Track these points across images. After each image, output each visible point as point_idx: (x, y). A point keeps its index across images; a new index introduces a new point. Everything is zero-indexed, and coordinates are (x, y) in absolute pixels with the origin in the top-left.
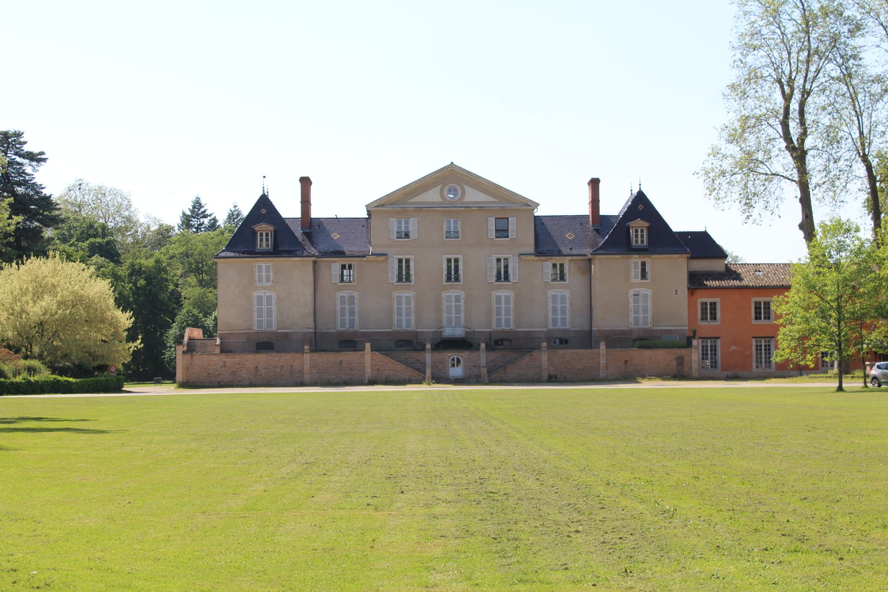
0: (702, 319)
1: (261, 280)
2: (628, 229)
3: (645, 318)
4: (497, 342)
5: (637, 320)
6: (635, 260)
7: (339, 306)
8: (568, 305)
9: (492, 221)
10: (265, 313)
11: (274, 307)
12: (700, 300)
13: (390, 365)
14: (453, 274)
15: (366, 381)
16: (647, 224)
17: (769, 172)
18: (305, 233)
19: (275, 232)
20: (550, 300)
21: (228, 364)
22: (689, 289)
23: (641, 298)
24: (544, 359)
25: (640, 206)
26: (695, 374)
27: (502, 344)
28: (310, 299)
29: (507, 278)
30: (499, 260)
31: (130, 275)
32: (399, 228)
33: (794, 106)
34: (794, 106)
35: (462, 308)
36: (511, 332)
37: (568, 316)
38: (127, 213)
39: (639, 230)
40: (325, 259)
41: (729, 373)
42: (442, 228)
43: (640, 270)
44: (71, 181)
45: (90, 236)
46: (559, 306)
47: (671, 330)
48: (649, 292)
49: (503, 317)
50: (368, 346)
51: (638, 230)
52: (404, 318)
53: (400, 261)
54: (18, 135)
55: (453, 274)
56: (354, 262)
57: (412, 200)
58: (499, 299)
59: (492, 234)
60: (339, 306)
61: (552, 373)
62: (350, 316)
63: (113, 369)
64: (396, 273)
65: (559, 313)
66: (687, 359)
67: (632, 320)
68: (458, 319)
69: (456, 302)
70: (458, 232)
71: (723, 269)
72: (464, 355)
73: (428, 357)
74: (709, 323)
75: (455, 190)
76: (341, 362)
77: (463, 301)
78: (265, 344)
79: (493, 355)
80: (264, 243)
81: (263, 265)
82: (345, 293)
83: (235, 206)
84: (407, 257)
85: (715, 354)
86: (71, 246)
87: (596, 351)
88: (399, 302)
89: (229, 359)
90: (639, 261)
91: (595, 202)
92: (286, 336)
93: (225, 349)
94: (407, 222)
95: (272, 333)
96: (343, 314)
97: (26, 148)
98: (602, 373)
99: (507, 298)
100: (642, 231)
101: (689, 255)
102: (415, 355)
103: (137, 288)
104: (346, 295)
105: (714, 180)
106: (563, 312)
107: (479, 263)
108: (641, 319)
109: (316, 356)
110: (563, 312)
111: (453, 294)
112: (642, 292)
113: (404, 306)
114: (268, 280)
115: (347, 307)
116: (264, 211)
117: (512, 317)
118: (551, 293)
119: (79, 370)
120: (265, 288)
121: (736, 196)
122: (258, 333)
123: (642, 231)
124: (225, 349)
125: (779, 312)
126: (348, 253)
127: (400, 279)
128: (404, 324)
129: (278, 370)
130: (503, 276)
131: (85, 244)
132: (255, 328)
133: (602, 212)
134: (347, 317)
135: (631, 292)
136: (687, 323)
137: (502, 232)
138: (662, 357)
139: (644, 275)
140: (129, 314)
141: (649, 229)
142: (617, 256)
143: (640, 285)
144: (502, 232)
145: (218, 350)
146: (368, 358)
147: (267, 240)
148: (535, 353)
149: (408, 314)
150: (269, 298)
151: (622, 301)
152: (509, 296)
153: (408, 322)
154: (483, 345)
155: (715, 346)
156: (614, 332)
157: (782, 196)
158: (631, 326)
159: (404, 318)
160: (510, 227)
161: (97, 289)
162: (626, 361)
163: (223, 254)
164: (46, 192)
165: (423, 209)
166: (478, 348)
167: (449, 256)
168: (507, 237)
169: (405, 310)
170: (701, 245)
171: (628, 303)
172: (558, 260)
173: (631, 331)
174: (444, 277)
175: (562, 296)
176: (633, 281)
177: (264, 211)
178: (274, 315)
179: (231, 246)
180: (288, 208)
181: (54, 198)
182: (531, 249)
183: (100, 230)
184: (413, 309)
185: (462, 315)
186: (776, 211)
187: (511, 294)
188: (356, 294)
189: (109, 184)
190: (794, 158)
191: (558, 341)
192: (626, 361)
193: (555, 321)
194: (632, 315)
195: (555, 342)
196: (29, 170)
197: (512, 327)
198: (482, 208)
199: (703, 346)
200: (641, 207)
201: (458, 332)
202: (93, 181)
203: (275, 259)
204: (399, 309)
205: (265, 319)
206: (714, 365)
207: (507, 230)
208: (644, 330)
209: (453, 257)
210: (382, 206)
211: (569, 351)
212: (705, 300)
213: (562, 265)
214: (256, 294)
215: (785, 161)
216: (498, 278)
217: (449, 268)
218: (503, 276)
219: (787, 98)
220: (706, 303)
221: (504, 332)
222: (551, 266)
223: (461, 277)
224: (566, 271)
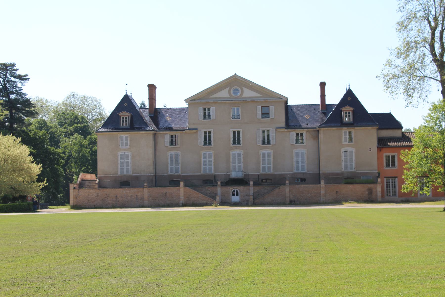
0: (387, 166)
1: (122, 145)
2: (341, 111)
3: (351, 166)
5: (346, 167)
6: (345, 130)
7: (169, 160)
8: (305, 158)
9: (259, 108)
11: (130, 161)
12: (385, 155)
13: (195, 195)
14: (236, 140)
15: (181, 204)
16: (352, 109)
17: (422, 75)
18: (151, 117)
19: (132, 117)
20: (295, 155)
21: (100, 195)
22: (378, 147)
23: (348, 154)
24: (287, 189)
25: (350, 98)
26: (380, 199)
28: (151, 156)
29: (268, 142)
30: (264, 132)
31: (89, 145)
33: (437, 34)
34: (437, 34)
35: (242, 160)
36: (271, 174)
37: (305, 165)
38: (98, 110)
40: (161, 132)
41: (403, 199)
42: (230, 113)
44: (69, 93)
45: (75, 123)
46: (300, 159)
47: (367, 173)
48: (354, 150)
49: (266, 165)
50: (182, 183)
51: (349, 112)
52: (208, 166)
53: (205, 133)
54: (13, 65)
56: (178, 134)
57: (212, 97)
58: (264, 155)
59: (260, 116)
60: (169, 160)
61: (292, 199)
62: (176, 165)
63: (29, 198)
65: (300, 163)
67: (343, 167)
68: (240, 167)
69: (238, 157)
70: (239, 115)
72: (240, 189)
73: (219, 190)
75: (238, 90)
77: (242, 156)
78: (125, 183)
79: (257, 188)
80: (124, 124)
81: (124, 136)
82: (173, 152)
83: (165, 106)
84: (210, 130)
85: (395, 187)
86: (65, 128)
87: (319, 185)
88: (205, 157)
89: (102, 192)
92: (137, 178)
93: (101, 186)
95: (129, 176)
97: (18, 73)
98: (323, 199)
100: (349, 113)
101: (378, 127)
102: (210, 189)
103: (93, 151)
105: (390, 80)
106: (303, 162)
107: (252, 133)
108: (349, 167)
109: (151, 189)
110: (303, 162)
111: (236, 152)
112: (349, 150)
113: (207, 160)
115: (174, 160)
116: (126, 104)
117: (272, 166)
118: (295, 151)
119: (5, 199)
120: (125, 150)
121: (402, 91)
122: (121, 176)
123: (349, 113)
124: (101, 186)
125: (405, 160)
126: (174, 129)
127: (205, 143)
128: (208, 170)
129: (129, 198)
130: (266, 141)
131: (72, 128)
132: (119, 173)
133: (327, 102)
134: (174, 166)
135: (343, 150)
136: (377, 168)
137: (265, 115)
138: (359, 189)
140: (40, 165)
141: (353, 112)
142: (334, 128)
143: (348, 146)
144: (265, 115)
145: (96, 187)
146: (182, 190)
147: (126, 121)
148: (282, 187)
149: (210, 164)
150: (127, 155)
151: (335, 155)
152: (270, 153)
153: (210, 169)
154: (251, 183)
155: (395, 182)
156: (332, 174)
157: (430, 90)
158: (343, 170)
159: (208, 166)
161: (18, 151)
162: (337, 192)
163: (101, 130)
164: (27, 97)
165: (217, 102)
167: (234, 130)
168: (269, 118)
169: (208, 161)
170: (387, 121)
171: (341, 156)
172: (299, 131)
173: (342, 173)
174: (231, 142)
175: (302, 153)
176: (344, 143)
177: (126, 104)
178: (130, 165)
179: (104, 126)
181: (33, 101)
182: (283, 125)
183: (81, 120)
185: (242, 165)
186: (426, 100)
187: (271, 152)
188: (179, 153)
189: (88, 94)
190: (437, 66)
191: (299, 179)
192: (337, 192)
193: (297, 168)
194: (343, 164)
195: (298, 180)
196: (19, 85)
197: (272, 172)
198: (253, 101)
200: (349, 99)
201: (240, 175)
202: (81, 92)
203: (130, 132)
204: (205, 161)
205: (125, 168)
206: (394, 194)
207: (269, 114)
208: (351, 173)
209: (236, 130)
210: (194, 100)
211: (302, 186)
212: (388, 154)
213: (302, 135)
214: (119, 153)
215: (432, 68)
216: (264, 142)
218: (266, 141)
219: (433, 30)
220: (389, 156)
221: (267, 174)
222: (295, 135)
223: (241, 142)
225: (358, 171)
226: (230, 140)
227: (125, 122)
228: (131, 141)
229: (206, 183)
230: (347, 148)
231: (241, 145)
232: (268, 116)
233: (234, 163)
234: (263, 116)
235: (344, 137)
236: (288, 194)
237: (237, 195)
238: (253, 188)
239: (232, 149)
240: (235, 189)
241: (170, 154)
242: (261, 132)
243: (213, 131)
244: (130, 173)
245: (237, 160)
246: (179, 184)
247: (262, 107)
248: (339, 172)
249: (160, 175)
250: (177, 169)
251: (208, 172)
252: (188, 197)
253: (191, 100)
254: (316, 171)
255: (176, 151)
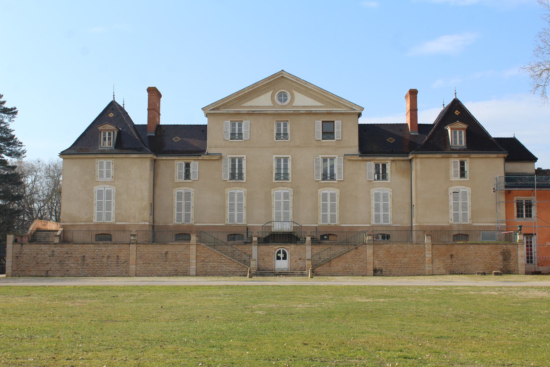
0: (518, 216)
1: (101, 176)
4: (322, 237)
5: (456, 216)
7: (176, 202)
10: (104, 207)
16: (465, 126)
19: (119, 133)
20: (373, 198)
21: (56, 253)
23: (460, 195)
25: (455, 112)
27: (328, 239)
29: (332, 177)
30: (325, 160)
32: (234, 130)
35: (291, 205)
36: (336, 227)
39: (456, 135)
40: (164, 158)
42: (273, 130)
43: (459, 169)
47: (489, 226)
48: (468, 190)
49: (329, 213)
50: (194, 238)
51: (453, 133)
53: (233, 160)
55: (282, 176)
57: (245, 105)
58: (325, 196)
60: (176, 202)
62: (186, 211)
64: (229, 171)
65: (381, 209)
66: (513, 254)
67: (451, 216)
71: (534, 172)
72: (289, 249)
73: (254, 250)
74: (523, 221)
75: (285, 96)
76: (167, 253)
77: (291, 198)
79: (318, 249)
88: (232, 199)
90: (458, 161)
91: (413, 111)
92: (123, 229)
94: (240, 125)
95: (110, 225)
96: (179, 209)
97: (5, 106)
99: (333, 196)
101: (506, 155)
104: (183, 191)
106: (386, 209)
111: (281, 191)
112: (461, 190)
113: (236, 202)
114: (108, 175)
115: (183, 202)
118: (374, 191)
120: (105, 183)
122: (97, 225)
123: (460, 133)
127: (233, 176)
132: (95, 221)
135: (452, 189)
137: (328, 134)
139: (463, 175)
143: (460, 183)
144: (328, 134)
145: (57, 240)
147: (109, 139)
149: (240, 210)
150: (109, 193)
152: (335, 194)
153: (240, 217)
155: (531, 242)
158: (452, 222)
160: (335, 130)
162: (452, 256)
164: (13, 133)
166: (303, 242)
168: (334, 139)
171: (448, 200)
172: (381, 160)
173: (451, 226)
176: (453, 179)
177: (111, 115)
178: (113, 208)
180: (139, 116)
184: (244, 204)
185: (291, 211)
187: (337, 191)
188: (192, 190)
191: (380, 236)
192: (452, 256)
193: (377, 217)
194: (452, 211)
196: (6, 121)
197: (337, 223)
199: (527, 242)
200: (457, 113)
201: (287, 227)
204: (232, 205)
205: (104, 211)
207: (333, 133)
210: (218, 108)
213: (384, 166)
217: (279, 168)
218: (328, 176)
221: (329, 227)
222: (373, 166)
224: (388, 171)
225: (475, 224)
226: (272, 173)
227: (107, 142)
228: (115, 169)
229: (234, 239)
230: (458, 187)
231: (290, 181)
232: (332, 137)
233: (278, 208)
234: (325, 137)
235: (453, 169)
236: (370, 259)
237: (285, 258)
238: (310, 247)
239: (274, 186)
240: (282, 249)
241: (178, 193)
242: (321, 161)
243: (245, 158)
244: (112, 221)
245: (282, 204)
246: (190, 239)
247: (323, 122)
248: (444, 225)
249: (161, 224)
250: (188, 216)
251: (236, 221)
252: (203, 261)
253: (213, 109)
254: (406, 223)
255: (187, 188)
